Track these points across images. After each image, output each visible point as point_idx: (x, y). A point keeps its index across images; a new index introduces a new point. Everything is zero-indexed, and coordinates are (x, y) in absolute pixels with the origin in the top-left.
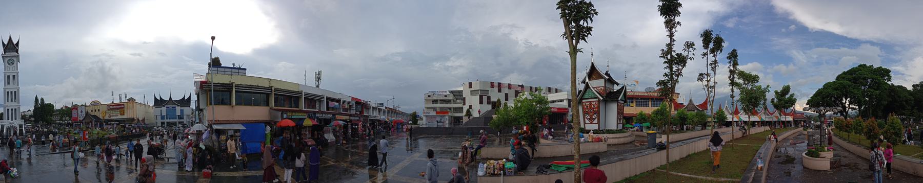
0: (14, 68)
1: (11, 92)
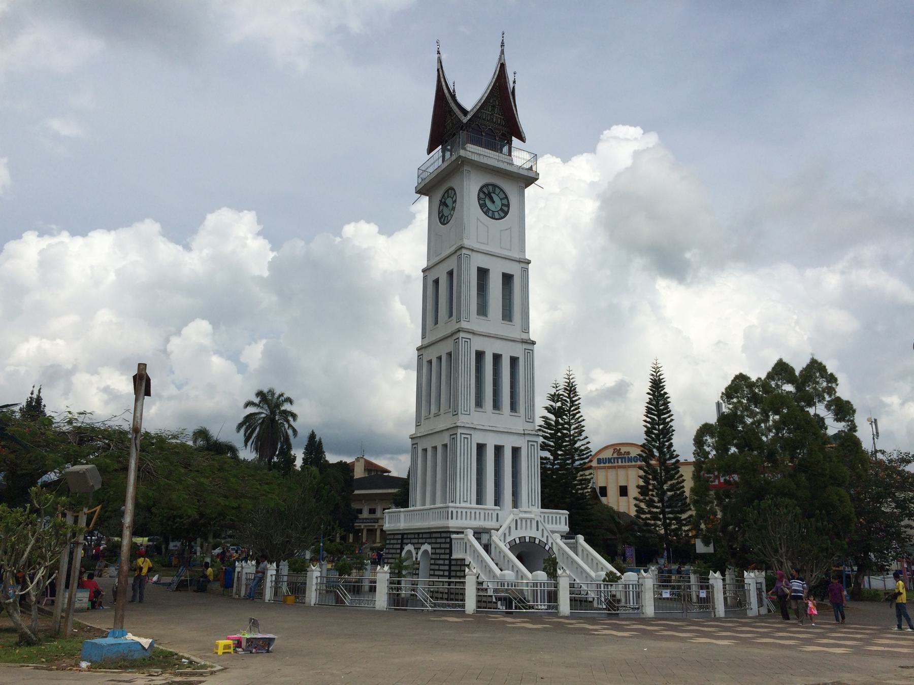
1: (497, 358)
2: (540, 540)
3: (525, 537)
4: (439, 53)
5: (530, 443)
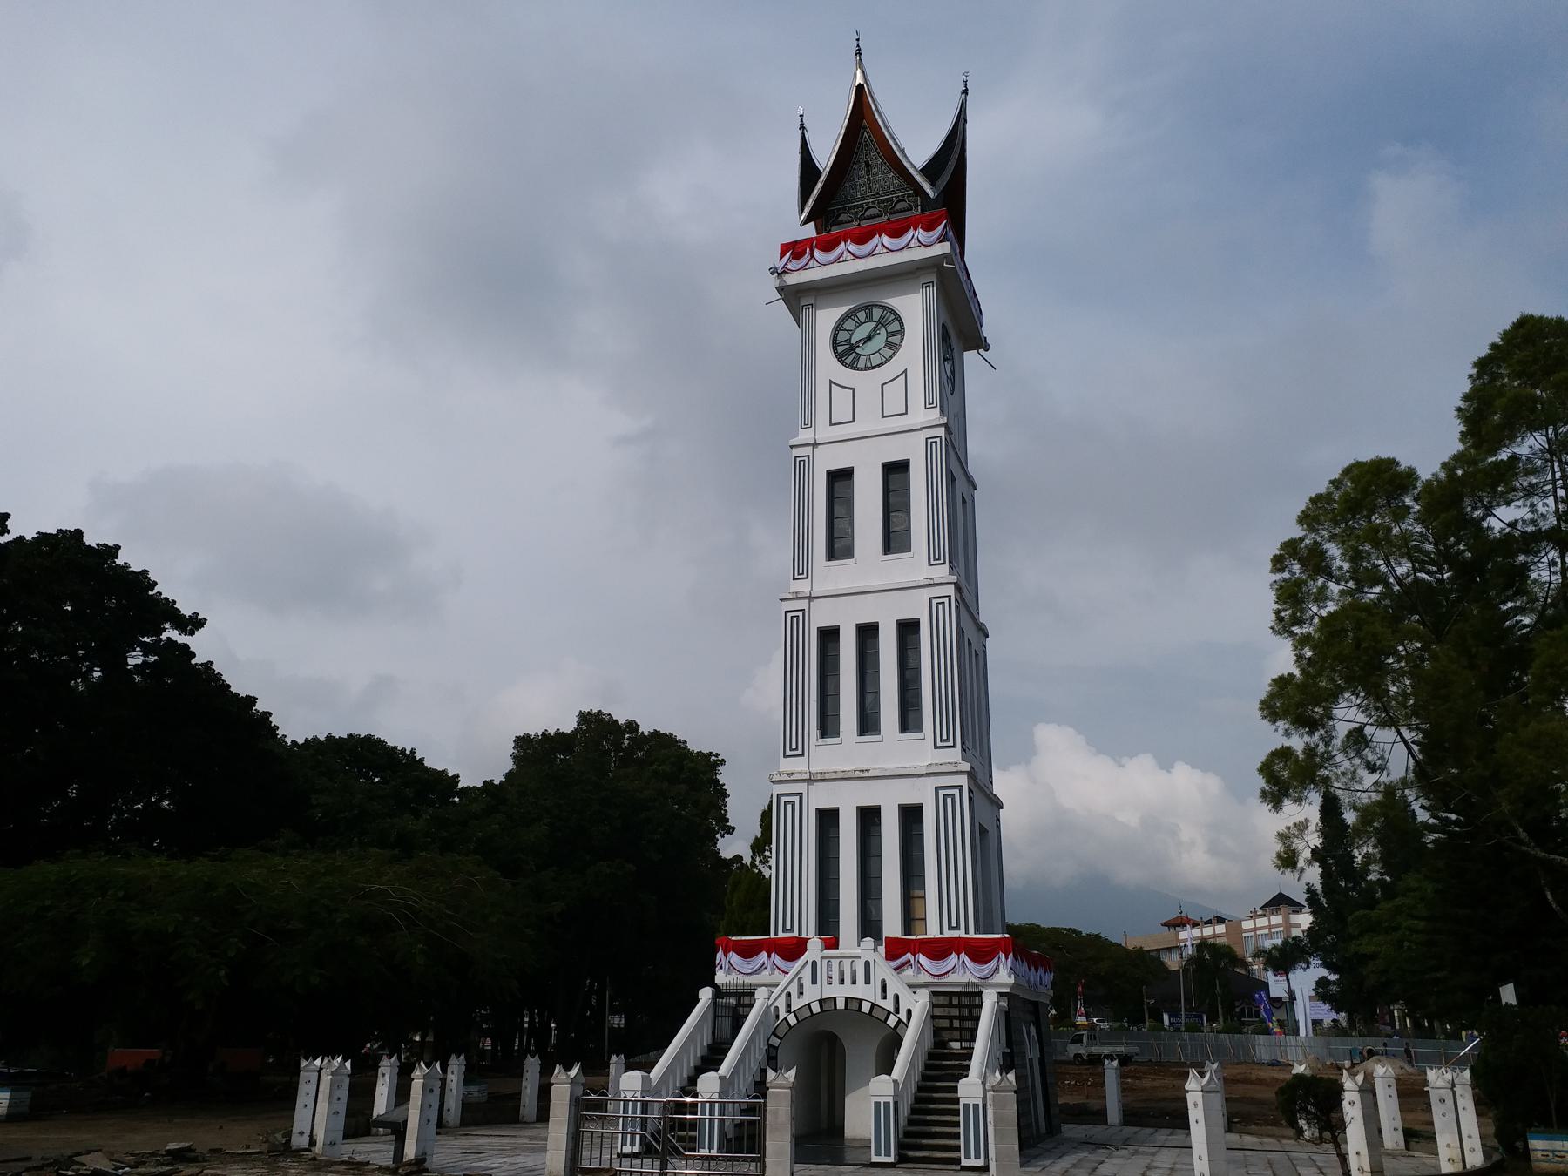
0: (895, 393)
1: (867, 633)
2: (873, 1005)
3: (835, 998)
4: (802, 127)
5: (941, 793)
